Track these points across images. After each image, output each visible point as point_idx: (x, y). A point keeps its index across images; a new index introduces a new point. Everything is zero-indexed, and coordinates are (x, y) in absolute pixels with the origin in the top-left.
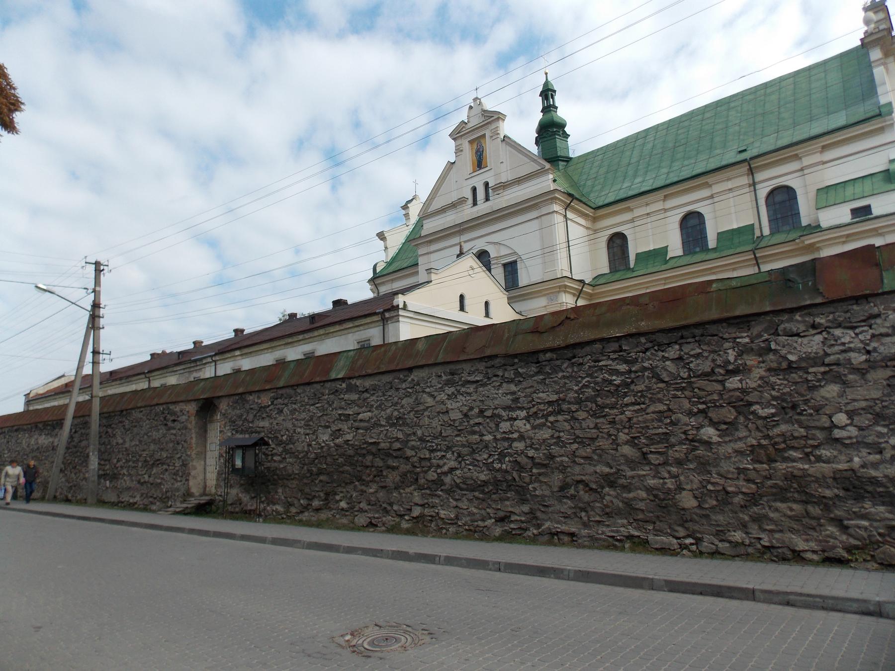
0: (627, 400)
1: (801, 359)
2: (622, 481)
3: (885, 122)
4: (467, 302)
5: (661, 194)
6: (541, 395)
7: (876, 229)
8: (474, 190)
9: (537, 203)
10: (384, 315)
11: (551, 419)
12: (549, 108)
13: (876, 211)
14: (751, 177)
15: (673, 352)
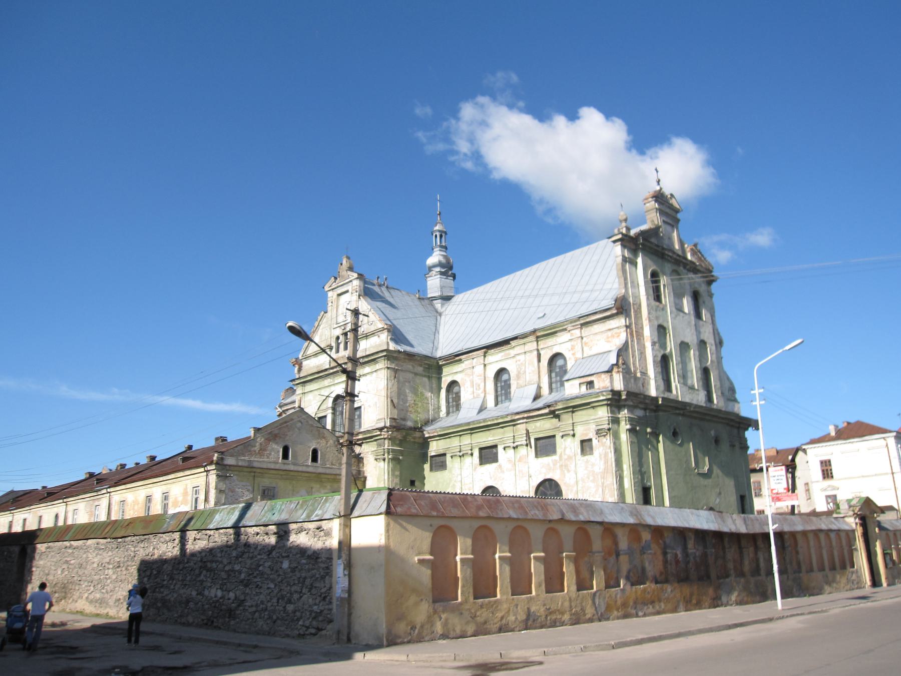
6: (116, 558)
11: (117, 570)
15: (142, 545)
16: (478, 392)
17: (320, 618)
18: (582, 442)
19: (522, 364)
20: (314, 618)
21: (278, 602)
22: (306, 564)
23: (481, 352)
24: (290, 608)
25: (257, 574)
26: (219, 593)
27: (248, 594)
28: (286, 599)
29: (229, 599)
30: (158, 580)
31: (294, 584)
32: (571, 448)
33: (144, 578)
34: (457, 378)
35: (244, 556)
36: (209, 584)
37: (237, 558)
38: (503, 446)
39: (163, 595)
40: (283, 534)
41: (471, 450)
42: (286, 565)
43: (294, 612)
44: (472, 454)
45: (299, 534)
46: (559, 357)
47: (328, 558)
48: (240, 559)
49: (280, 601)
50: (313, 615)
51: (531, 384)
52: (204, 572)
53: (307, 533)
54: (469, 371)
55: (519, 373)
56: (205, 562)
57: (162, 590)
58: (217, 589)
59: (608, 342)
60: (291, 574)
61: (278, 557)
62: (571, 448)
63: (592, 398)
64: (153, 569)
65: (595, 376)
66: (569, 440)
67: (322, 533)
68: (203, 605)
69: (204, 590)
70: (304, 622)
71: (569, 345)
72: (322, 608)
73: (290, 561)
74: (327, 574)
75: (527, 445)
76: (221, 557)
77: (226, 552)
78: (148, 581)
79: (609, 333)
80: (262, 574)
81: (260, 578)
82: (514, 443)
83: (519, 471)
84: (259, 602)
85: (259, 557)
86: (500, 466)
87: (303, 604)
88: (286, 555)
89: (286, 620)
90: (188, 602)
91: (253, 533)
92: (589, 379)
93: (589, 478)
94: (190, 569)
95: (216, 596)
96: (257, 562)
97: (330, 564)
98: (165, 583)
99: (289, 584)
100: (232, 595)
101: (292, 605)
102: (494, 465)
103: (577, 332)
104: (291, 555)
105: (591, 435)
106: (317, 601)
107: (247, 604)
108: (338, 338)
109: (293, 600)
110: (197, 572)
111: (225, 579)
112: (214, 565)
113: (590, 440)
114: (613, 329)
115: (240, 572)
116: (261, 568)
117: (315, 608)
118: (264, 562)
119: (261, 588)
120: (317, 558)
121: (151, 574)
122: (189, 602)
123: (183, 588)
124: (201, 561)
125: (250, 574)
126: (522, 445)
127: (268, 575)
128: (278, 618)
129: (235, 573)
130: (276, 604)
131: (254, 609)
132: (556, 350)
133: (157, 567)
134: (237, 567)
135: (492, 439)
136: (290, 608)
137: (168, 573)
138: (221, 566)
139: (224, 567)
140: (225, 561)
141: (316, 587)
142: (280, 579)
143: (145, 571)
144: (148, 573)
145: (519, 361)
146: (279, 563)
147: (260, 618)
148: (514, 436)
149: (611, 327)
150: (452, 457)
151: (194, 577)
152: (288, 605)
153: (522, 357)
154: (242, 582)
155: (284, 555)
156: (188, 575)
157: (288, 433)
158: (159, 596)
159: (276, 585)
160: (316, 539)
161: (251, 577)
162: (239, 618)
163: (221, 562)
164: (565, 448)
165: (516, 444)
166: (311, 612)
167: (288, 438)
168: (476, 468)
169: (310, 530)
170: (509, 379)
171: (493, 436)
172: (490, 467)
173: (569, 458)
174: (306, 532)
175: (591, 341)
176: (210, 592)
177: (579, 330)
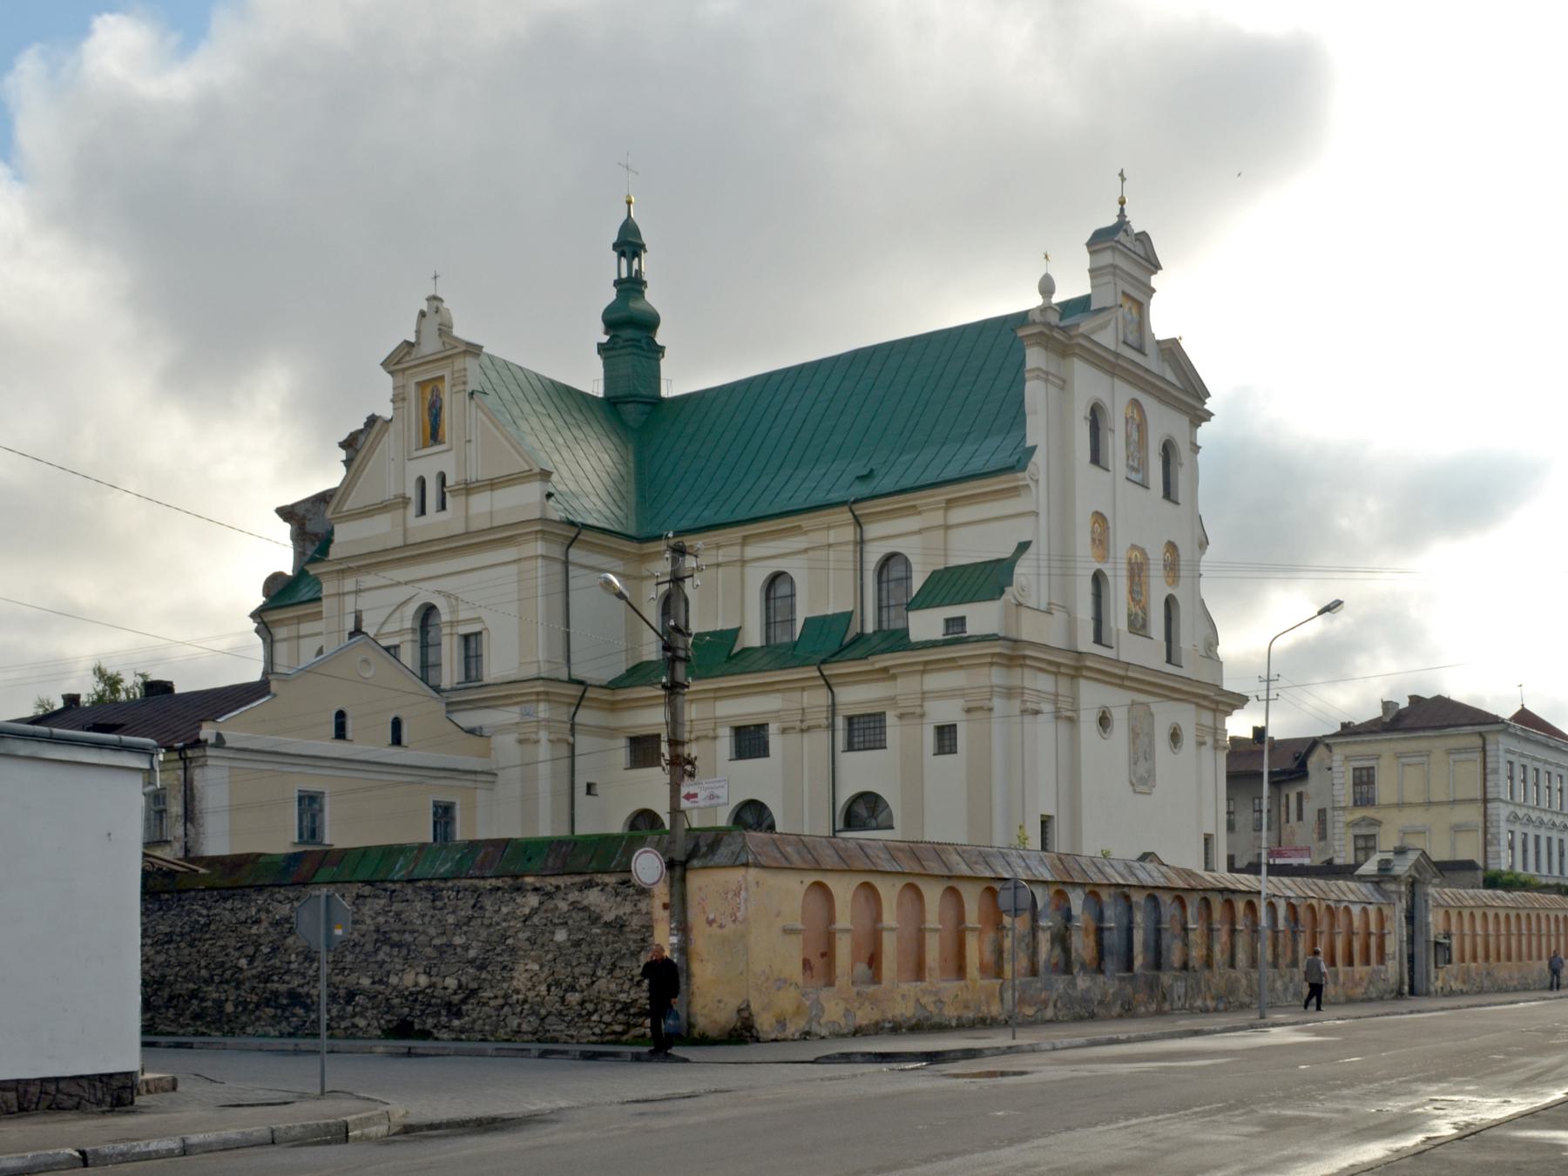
0: (208, 936)
1: (281, 919)
2: (201, 995)
3: (1017, 480)
4: (350, 725)
5: (737, 533)
6: (161, 927)
7: (953, 659)
8: (422, 482)
9: (512, 536)
10: (185, 753)
11: (166, 946)
12: (631, 286)
13: (971, 629)
14: (858, 530)
15: (229, 905)
17: (632, 1011)
20: (618, 1012)
21: (549, 990)
22: (603, 935)
24: (574, 998)
25: (503, 950)
26: (423, 980)
27: (485, 980)
28: (564, 985)
29: (445, 988)
30: (276, 962)
31: (579, 964)
33: (239, 958)
35: (471, 924)
36: (399, 967)
37: (457, 926)
39: (290, 986)
40: (553, 890)
42: (561, 936)
43: (582, 1003)
45: (586, 892)
47: (643, 926)
48: (465, 928)
49: (553, 989)
50: (618, 1006)
52: (386, 949)
53: (602, 890)
56: (385, 932)
57: (287, 978)
58: (417, 974)
60: (573, 950)
61: (546, 925)
64: (261, 945)
67: (631, 891)
68: (387, 1000)
69: (388, 976)
70: (601, 1017)
72: (635, 997)
73: (569, 930)
74: (642, 949)
76: (424, 924)
77: (432, 917)
78: (248, 965)
80: (513, 950)
81: (511, 955)
82: (802, 721)
84: (510, 991)
85: (504, 924)
87: (599, 992)
88: (561, 921)
89: (567, 1015)
90: (351, 996)
91: (489, 887)
94: (352, 944)
95: (416, 984)
96: (502, 932)
97: (647, 934)
98: (293, 966)
99: (568, 964)
100: (451, 982)
101: (577, 994)
104: (570, 922)
106: (626, 987)
107: (484, 994)
109: (577, 987)
110: (369, 947)
111: (434, 958)
112: (408, 937)
115: (466, 948)
116: (510, 941)
117: (623, 997)
118: (516, 932)
119: (511, 970)
120: (622, 926)
121: (255, 953)
122: (356, 994)
123: (337, 974)
124: (377, 931)
125: (488, 951)
126: (819, 726)
127: (525, 951)
128: (549, 1013)
129: (455, 949)
130: (545, 993)
131: (500, 1001)
133: (270, 942)
134: (458, 940)
136: (574, 998)
137: (301, 949)
138: (422, 938)
139: (431, 940)
140: (432, 931)
141: (622, 968)
142: (550, 956)
143: (241, 947)
144: (250, 950)
146: (547, 934)
147: (513, 1014)
148: (803, 709)
151: (362, 957)
152: (569, 994)
154: (471, 962)
155: (556, 921)
156: (347, 953)
158: (283, 988)
159: (542, 966)
160: (619, 899)
161: (490, 953)
162: (468, 1016)
163: (425, 933)
166: (614, 1002)
169: (607, 885)
174: (599, 888)
176: (401, 979)
177: (941, 512)
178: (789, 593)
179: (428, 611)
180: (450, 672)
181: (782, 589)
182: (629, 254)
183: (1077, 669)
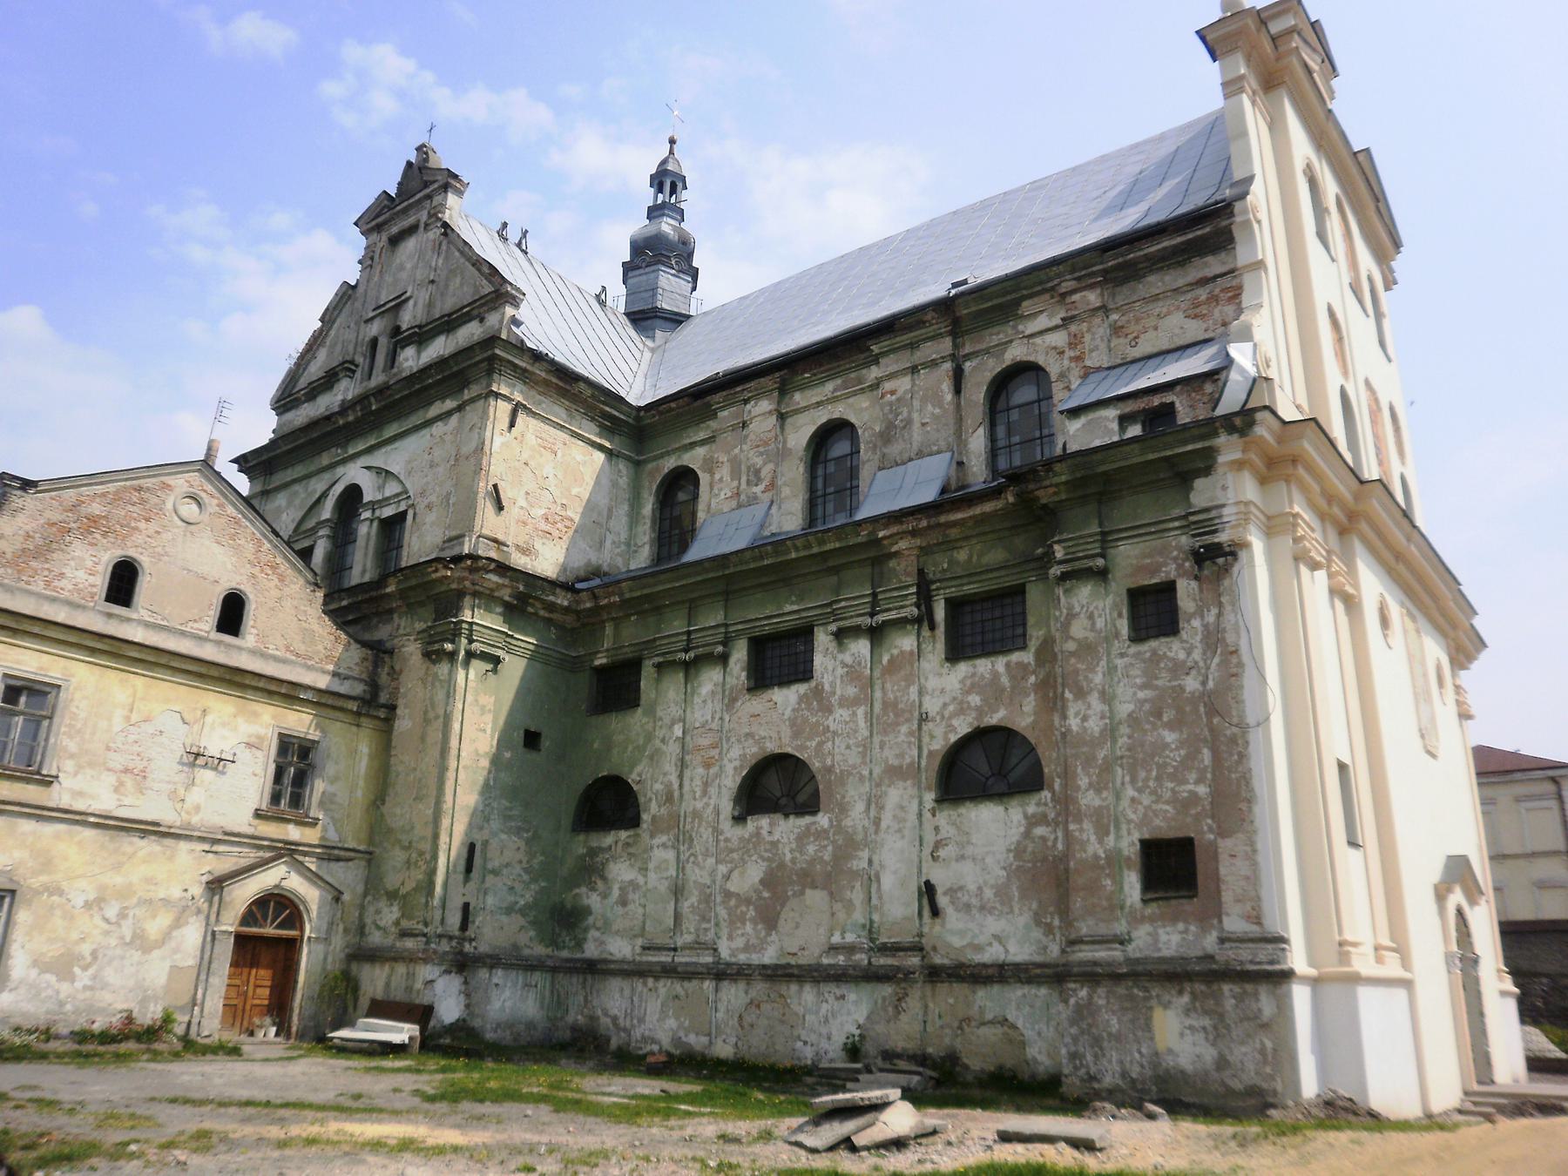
16: (755, 489)
18: (1137, 597)
19: (898, 400)
23: (768, 382)
32: (1091, 617)
34: (693, 459)
38: (833, 627)
41: (725, 643)
44: (724, 659)
46: (1032, 374)
51: (930, 455)
54: (728, 437)
55: (890, 426)
59: (1196, 316)
62: (1091, 617)
63: (1185, 442)
65: (1178, 388)
66: (1084, 593)
71: (1059, 339)
75: (918, 621)
79: (1202, 294)
82: (872, 615)
83: (885, 704)
86: (818, 692)
92: (1156, 401)
93: (1159, 715)
102: (802, 688)
103: (1093, 298)
105: (1169, 571)
108: (374, 343)
113: (1169, 588)
114: (1216, 277)
132: (1016, 352)
135: (795, 607)
145: (893, 393)
148: (874, 595)
149: (1209, 272)
150: (659, 666)
153: (904, 384)
157: (142, 525)
164: (1071, 616)
165: (881, 618)
167: (139, 538)
168: (733, 700)
170: (855, 452)
171: (801, 599)
172: (786, 698)
173: (1087, 649)
175: (1138, 320)
178: (849, 451)
179: (352, 495)
180: (361, 567)
181: (840, 448)
182: (667, 188)
183: (1352, 516)
